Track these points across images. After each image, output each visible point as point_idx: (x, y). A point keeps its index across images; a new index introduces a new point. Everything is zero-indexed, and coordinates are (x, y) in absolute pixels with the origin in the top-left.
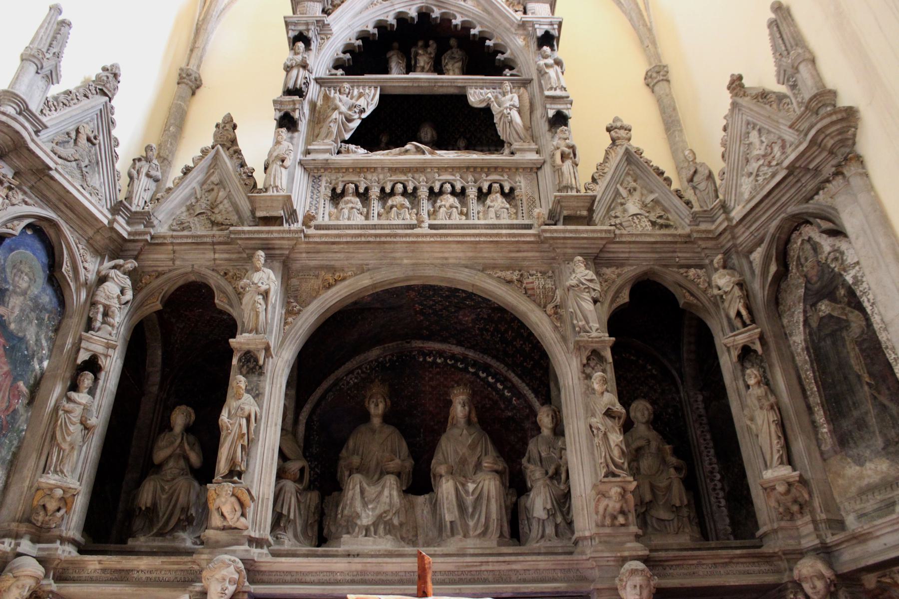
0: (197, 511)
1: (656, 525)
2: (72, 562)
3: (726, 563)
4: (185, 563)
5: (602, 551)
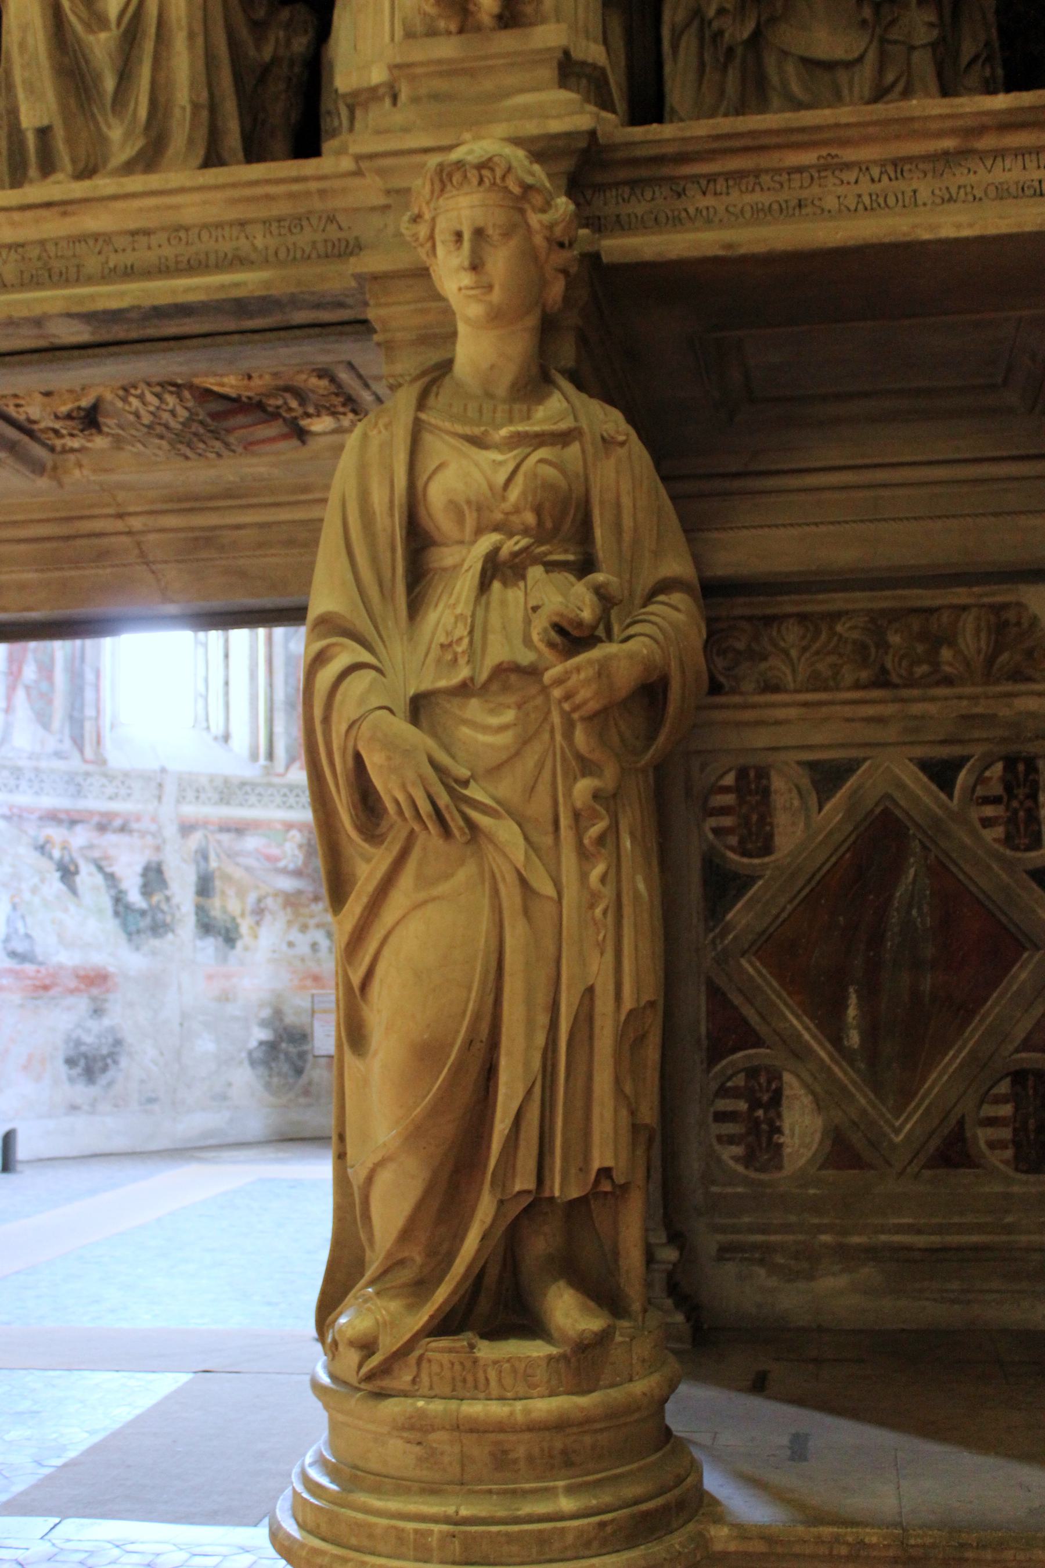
1: (796, 88)
3: (946, 153)
5: (406, 130)
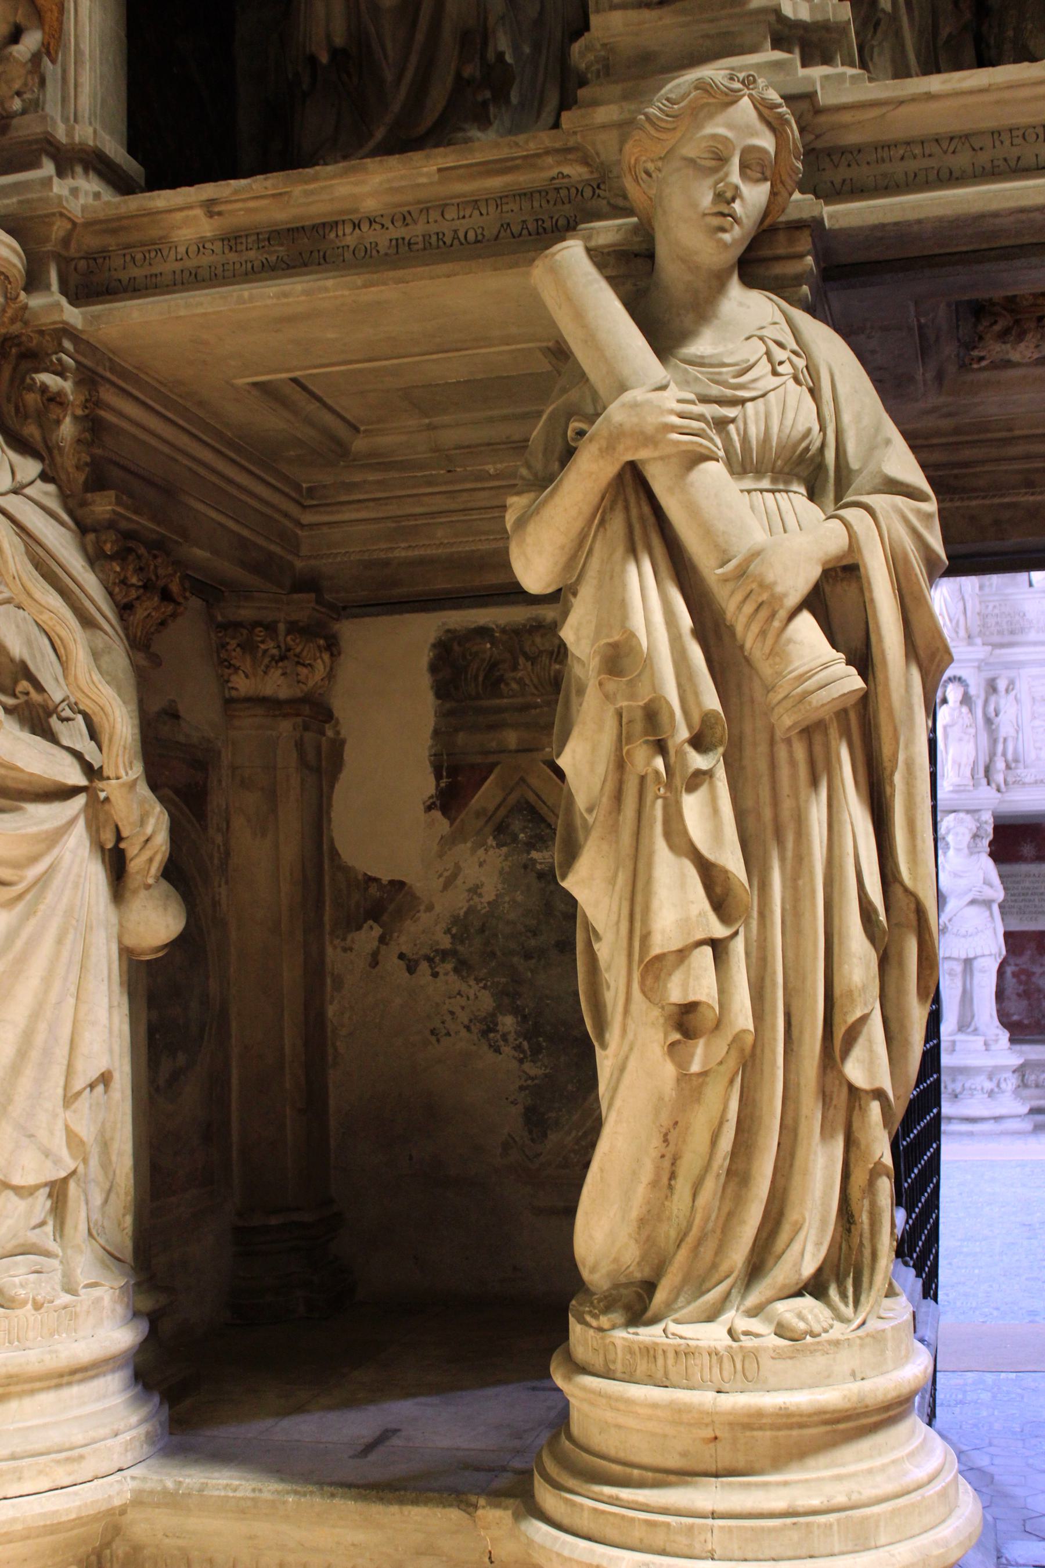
0: (516, 48)
2: (111, 226)
4: (530, 161)
